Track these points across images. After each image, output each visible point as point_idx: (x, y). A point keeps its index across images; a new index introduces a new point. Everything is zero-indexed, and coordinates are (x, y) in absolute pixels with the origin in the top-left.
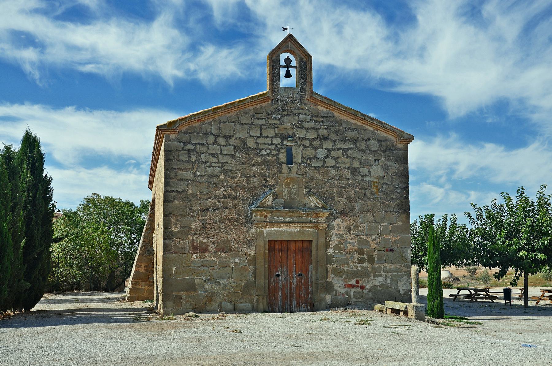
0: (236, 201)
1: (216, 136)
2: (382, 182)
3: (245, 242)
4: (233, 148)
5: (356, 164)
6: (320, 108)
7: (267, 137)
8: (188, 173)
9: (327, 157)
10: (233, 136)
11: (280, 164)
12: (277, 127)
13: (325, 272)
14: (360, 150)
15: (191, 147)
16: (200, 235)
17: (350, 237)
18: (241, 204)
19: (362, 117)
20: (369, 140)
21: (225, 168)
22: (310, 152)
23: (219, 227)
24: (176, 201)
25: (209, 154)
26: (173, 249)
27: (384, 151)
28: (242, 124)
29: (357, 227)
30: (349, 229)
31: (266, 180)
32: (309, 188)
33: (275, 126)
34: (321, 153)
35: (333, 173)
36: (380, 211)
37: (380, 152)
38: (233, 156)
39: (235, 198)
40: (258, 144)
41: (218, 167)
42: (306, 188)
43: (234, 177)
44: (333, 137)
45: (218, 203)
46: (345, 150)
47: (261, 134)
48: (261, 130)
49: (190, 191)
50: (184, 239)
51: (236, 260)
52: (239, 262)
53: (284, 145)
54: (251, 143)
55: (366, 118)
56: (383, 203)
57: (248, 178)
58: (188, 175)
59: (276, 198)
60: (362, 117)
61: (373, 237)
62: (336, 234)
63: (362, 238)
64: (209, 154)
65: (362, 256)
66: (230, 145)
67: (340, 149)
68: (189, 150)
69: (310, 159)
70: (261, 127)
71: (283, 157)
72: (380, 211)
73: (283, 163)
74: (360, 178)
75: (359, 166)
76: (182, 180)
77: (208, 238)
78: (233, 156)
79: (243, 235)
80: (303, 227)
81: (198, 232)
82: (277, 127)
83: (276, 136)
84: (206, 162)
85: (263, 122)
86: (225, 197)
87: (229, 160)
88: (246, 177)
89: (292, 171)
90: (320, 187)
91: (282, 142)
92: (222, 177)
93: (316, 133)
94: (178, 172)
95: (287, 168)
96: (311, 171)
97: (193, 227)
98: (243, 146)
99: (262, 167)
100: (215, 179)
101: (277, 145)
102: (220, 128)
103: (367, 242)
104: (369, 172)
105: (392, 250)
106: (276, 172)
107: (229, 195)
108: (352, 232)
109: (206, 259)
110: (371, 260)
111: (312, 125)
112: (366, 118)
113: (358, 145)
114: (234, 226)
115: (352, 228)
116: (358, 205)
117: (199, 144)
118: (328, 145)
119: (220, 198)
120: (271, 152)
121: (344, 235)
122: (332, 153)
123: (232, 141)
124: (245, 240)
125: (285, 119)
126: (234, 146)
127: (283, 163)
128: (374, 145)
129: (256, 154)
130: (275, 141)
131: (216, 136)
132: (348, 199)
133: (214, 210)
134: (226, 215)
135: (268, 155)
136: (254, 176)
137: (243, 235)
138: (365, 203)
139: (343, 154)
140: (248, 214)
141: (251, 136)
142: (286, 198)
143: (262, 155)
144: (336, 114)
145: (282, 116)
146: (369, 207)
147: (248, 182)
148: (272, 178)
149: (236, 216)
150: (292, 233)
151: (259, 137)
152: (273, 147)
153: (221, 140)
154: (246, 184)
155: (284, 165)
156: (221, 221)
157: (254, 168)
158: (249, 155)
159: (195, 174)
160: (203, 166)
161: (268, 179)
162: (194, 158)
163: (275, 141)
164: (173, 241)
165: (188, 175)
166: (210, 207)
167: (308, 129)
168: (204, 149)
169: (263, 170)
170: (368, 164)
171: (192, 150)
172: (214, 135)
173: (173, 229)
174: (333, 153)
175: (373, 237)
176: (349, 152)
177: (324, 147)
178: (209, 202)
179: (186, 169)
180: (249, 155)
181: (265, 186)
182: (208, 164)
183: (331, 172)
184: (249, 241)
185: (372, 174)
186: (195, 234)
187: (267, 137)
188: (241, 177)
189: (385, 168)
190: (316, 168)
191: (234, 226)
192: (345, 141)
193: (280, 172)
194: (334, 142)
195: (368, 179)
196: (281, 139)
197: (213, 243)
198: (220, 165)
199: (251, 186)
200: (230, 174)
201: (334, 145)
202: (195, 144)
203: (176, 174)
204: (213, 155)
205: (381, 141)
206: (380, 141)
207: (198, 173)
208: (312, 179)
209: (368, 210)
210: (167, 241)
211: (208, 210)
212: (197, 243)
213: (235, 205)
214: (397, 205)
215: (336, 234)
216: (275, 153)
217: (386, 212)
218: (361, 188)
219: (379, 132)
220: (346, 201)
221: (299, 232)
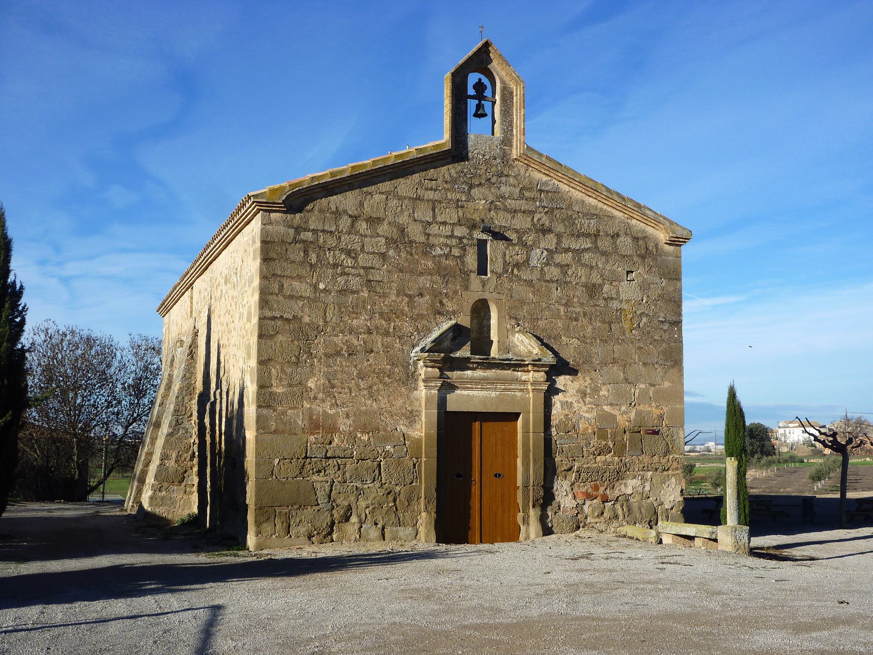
0: (389, 339)
1: (355, 218)
2: (638, 312)
3: (403, 414)
4: (384, 241)
5: (596, 279)
6: (538, 176)
7: (444, 223)
8: (304, 286)
9: (547, 264)
10: (384, 220)
11: (467, 274)
12: (462, 207)
13: (542, 471)
14: (604, 254)
15: (308, 236)
16: (323, 401)
17: (585, 408)
18: (398, 345)
19: (608, 195)
20: (618, 236)
21: (371, 277)
22: (516, 254)
23: (358, 385)
24: (280, 338)
25: (342, 250)
26: (273, 425)
27: (643, 257)
28: (400, 198)
29: (596, 390)
30: (584, 394)
31: (441, 302)
33: (458, 204)
34: (537, 256)
35: (556, 294)
36: (635, 363)
37: (635, 259)
38: (383, 256)
39: (387, 334)
40: (428, 235)
41: (359, 275)
42: (510, 318)
43: (385, 296)
44: (560, 228)
45: (355, 342)
46: (578, 252)
47: (434, 216)
48: (433, 210)
49: (306, 319)
50: (295, 408)
51: (388, 448)
52: (392, 450)
53: (473, 239)
54: (415, 232)
55: (615, 197)
56: (640, 348)
57: (410, 297)
58: (302, 288)
60: (608, 195)
61: (623, 408)
62: (561, 402)
63: (604, 410)
64: (342, 250)
65: (604, 443)
66: (378, 235)
67: (567, 250)
68: (304, 242)
69: (517, 265)
70: (434, 205)
71: (471, 261)
72: (635, 363)
73: (471, 272)
74: (602, 302)
75: (600, 281)
76: (291, 297)
77: (337, 405)
78: (383, 256)
79: (400, 402)
80: (505, 390)
81: (321, 395)
82: (462, 207)
83: (459, 223)
84: (335, 266)
85: (436, 196)
86: (369, 332)
87: (376, 262)
88: (406, 295)
89: (487, 287)
90: (535, 317)
91: (471, 234)
92: (365, 294)
93: (529, 219)
94: (284, 281)
95: (478, 281)
96: (520, 288)
97: (311, 384)
98: (400, 239)
99: (434, 278)
100: (351, 298)
101: (461, 239)
102: (361, 204)
103: (614, 417)
104: (618, 292)
105: (656, 433)
107: (377, 327)
108: (588, 399)
109: (334, 444)
110: (620, 451)
111: (524, 205)
112: (615, 197)
113: (599, 244)
114: (385, 384)
115: (588, 391)
116: (598, 350)
117: (323, 231)
118: (550, 241)
119: (361, 333)
120: (450, 251)
121: (575, 405)
122: (556, 256)
123: (383, 228)
124: (404, 411)
125: (475, 192)
126: (387, 238)
127: (471, 272)
128: (625, 243)
129: (425, 254)
130: (459, 231)
131: (355, 218)
132: (583, 339)
133: (350, 355)
134: (370, 365)
135: (447, 256)
136: (421, 295)
137: (400, 402)
138: (610, 348)
139: (574, 259)
140: (409, 364)
141: (415, 221)
143: (434, 257)
144: (564, 188)
145: (471, 187)
146: (616, 355)
149: (389, 367)
150: (484, 400)
151: (429, 224)
152: (454, 242)
153: (363, 226)
154: (406, 309)
155: (473, 276)
156: (361, 376)
157: (421, 279)
158: (411, 254)
159: (315, 287)
160: (330, 271)
162: (313, 258)
163: (459, 231)
164: (274, 411)
165: (302, 288)
166: (342, 349)
167: (515, 211)
168: (332, 242)
169: (436, 283)
170: (614, 279)
171: (312, 242)
172: (351, 216)
173: (274, 389)
174: (559, 258)
175: (623, 408)
176: (587, 256)
177: (542, 245)
178: (339, 340)
179: (300, 278)
180: (411, 254)
181: (439, 313)
182: (339, 270)
183: (554, 290)
184: (411, 412)
185: (623, 296)
186: (315, 398)
187: (444, 223)
188: (398, 295)
189: (644, 287)
190: (530, 283)
191: (385, 384)
192: (578, 236)
193: (467, 288)
194: (559, 236)
195: (615, 305)
196: (468, 227)
197: (348, 416)
198: (362, 271)
199: (416, 312)
200: (378, 289)
201: (559, 242)
202: (315, 231)
203: (281, 287)
204: (349, 253)
205: (638, 239)
206: (636, 239)
207: (322, 286)
208: (522, 302)
209: (615, 361)
210: (265, 411)
211: (338, 353)
212: (319, 416)
213: (387, 347)
214: (664, 353)
215: (561, 402)
216: (456, 252)
217: (645, 364)
218: (604, 322)
219: (634, 222)
220: (579, 343)
221: (497, 397)
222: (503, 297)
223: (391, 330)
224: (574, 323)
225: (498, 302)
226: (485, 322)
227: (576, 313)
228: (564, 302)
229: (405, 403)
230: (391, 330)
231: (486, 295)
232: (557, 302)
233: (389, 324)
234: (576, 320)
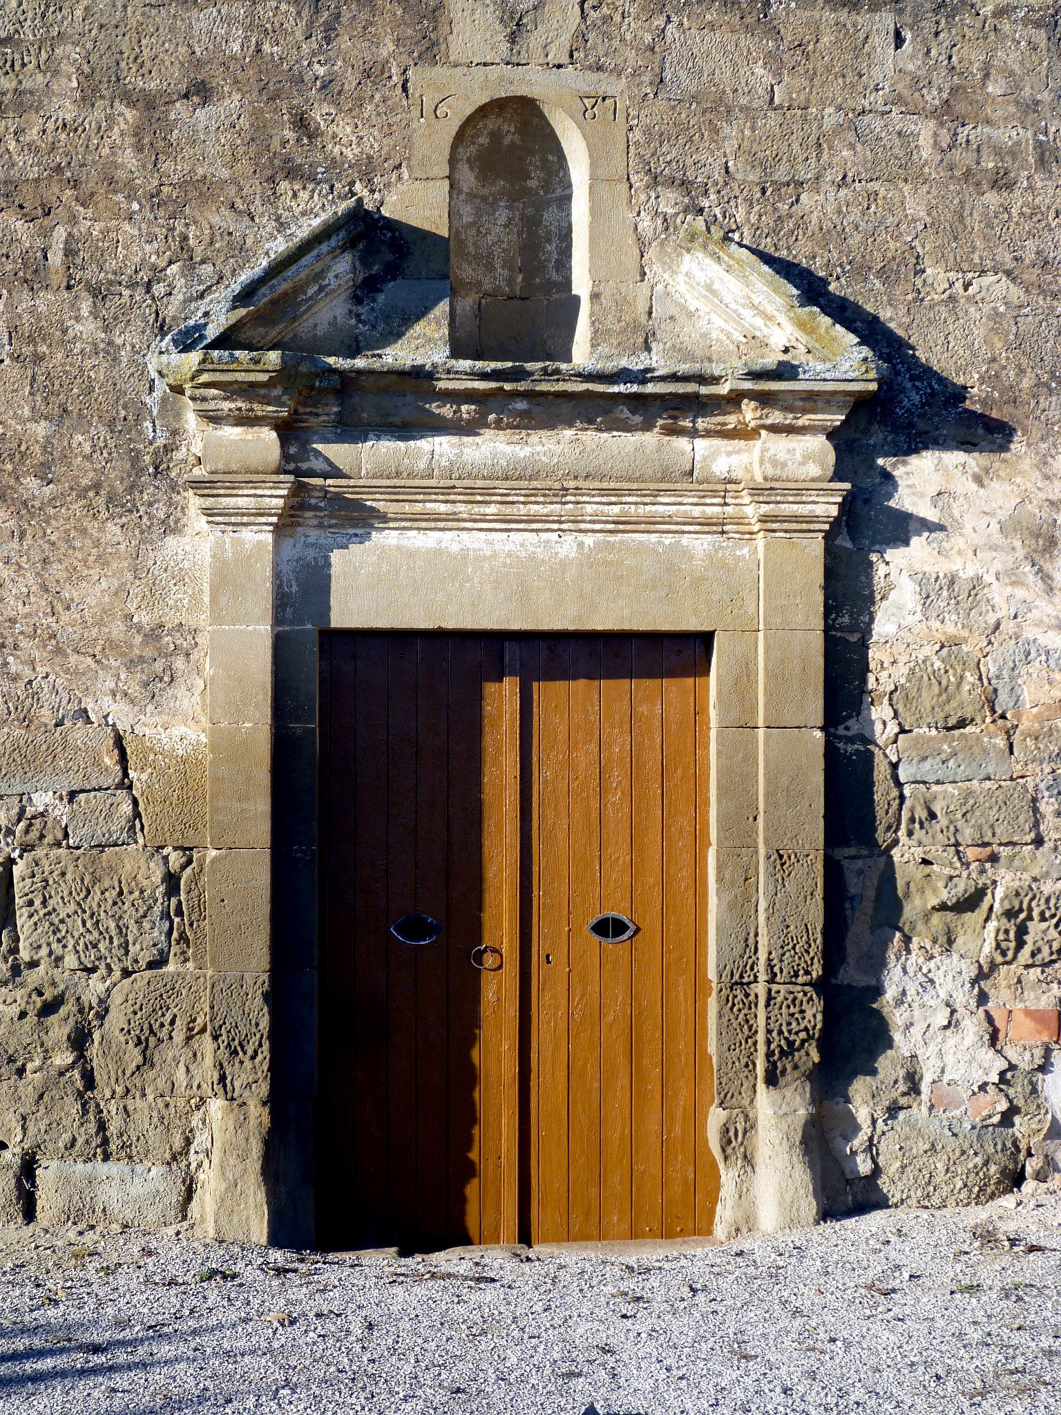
0: (45, 301)
3: (111, 645)
13: (815, 913)
18: (87, 328)
31: (301, 123)
32: (685, 185)
42: (655, 181)
52: (61, 811)
57: (149, 103)
59: (393, 271)
62: (922, 580)
79: (94, 592)
80: (623, 524)
88: (129, 98)
89: (534, 40)
90: (781, 174)
96: (702, 42)
106: (388, 48)
121: (998, 593)
124: (117, 629)
136: (201, 92)
140: (141, 412)
142: (499, 278)
147: (153, 135)
148: (360, 102)
149: (41, 429)
154: (128, 158)
161: (319, 114)
169: (276, 33)
181: (292, 172)
184: (153, 634)
188: (87, 97)
193: (430, 50)
199: (174, 168)
215: (922, 580)
220: (1016, 293)
222: (616, 86)
223: (56, 258)
224: (992, 198)
225: (591, 106)
226: (550, 216)
227: (998, 152)
228: (933, 98)
229: (122, 592)
230: (56, 258)
231: (532, 82)
232: (899, 100)
233: (46, 233)
234: (1003, 182)
